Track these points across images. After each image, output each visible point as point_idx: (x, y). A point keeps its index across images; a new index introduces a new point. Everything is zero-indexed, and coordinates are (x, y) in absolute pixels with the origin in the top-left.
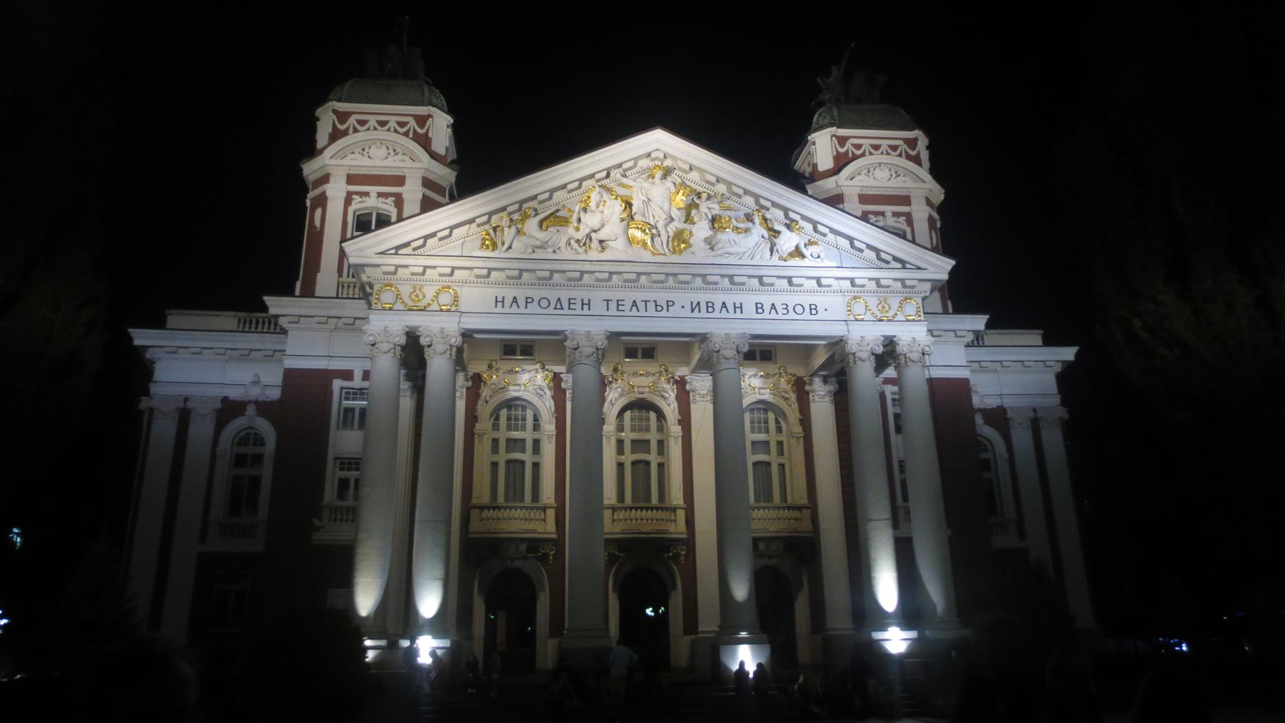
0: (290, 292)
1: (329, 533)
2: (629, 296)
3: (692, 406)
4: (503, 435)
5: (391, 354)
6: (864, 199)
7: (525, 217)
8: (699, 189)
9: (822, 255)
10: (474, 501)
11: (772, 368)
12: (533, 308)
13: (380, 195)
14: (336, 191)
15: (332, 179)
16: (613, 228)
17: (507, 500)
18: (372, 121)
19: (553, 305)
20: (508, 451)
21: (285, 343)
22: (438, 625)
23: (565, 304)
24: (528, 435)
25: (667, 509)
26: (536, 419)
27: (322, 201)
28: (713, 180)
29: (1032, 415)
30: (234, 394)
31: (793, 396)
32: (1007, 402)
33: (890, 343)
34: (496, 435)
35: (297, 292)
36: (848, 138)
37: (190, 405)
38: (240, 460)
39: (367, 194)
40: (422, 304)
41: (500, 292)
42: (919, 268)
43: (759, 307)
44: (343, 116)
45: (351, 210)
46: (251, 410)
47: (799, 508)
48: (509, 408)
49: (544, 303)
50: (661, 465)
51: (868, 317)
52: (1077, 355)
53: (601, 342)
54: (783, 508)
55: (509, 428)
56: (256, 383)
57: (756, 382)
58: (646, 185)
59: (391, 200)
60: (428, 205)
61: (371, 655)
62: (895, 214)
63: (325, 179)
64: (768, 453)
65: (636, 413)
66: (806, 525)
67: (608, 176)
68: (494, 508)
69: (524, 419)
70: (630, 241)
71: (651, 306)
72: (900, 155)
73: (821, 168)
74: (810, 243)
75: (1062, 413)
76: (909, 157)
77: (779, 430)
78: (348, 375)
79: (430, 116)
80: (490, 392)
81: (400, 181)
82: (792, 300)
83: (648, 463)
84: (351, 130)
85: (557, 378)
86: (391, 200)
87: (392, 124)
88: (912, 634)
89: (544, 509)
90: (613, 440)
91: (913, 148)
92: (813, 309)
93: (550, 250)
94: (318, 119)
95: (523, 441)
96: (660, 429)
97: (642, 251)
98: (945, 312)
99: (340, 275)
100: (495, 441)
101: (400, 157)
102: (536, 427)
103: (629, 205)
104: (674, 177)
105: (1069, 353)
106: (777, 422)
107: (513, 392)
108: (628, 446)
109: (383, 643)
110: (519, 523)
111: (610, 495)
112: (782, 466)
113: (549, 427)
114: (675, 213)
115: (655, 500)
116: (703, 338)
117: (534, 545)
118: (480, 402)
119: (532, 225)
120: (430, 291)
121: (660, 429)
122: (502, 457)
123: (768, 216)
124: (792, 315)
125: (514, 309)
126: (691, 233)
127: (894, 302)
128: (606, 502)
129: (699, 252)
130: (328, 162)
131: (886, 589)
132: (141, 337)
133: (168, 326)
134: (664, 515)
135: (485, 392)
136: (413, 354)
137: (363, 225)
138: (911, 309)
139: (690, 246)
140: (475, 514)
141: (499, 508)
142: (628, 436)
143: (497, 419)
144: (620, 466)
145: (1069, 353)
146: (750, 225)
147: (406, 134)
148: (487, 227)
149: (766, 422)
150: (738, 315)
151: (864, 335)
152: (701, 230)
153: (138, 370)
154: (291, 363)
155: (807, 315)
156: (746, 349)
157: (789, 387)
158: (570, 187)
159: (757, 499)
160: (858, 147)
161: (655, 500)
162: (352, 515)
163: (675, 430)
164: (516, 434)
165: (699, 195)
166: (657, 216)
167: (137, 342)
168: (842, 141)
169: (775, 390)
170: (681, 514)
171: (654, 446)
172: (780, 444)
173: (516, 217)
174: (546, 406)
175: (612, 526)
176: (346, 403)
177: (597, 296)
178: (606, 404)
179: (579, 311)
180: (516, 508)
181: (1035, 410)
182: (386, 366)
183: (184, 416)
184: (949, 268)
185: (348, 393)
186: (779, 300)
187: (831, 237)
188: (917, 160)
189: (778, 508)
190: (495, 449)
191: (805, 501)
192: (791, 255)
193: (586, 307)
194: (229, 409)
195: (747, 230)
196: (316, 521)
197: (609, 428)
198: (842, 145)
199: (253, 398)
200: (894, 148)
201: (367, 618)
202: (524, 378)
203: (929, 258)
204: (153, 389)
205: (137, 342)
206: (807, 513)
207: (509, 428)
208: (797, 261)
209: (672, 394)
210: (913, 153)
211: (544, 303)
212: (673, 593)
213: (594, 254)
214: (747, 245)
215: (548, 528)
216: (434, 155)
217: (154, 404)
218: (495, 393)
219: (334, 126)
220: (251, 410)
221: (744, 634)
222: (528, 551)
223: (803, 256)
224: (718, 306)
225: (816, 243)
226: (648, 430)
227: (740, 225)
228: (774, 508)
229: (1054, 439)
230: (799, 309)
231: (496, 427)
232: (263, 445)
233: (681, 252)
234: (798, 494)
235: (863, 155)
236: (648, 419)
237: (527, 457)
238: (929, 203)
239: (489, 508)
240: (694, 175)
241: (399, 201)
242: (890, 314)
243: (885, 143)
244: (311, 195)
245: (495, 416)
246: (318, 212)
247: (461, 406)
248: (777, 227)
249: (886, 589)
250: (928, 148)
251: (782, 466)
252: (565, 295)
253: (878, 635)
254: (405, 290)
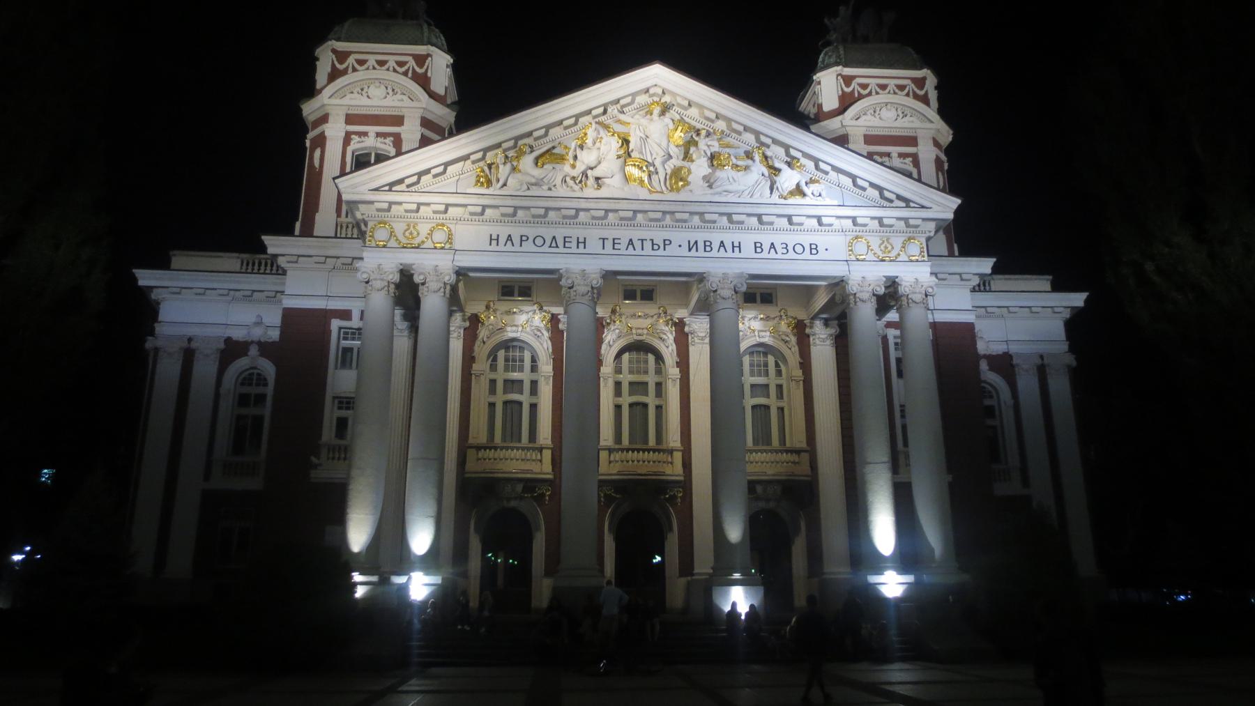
0: (289, 232)
1: (325, 471)
2: (625, 234)
3: (691, 349)
4: (500, 376)
5: (384, 292)
6: (869, 139)
7: (521, 154)
8: (699, 126)
9: (823, 194)
10: (471, 441)
11: (772, 310)
12: (528, 246)
13: (378, 135)
14: (335, 131)
15: (331, 119)
16: (610, 166)
17: (504, 440)
18: (372, 60)
19: (548, 243)
20: (505, 392)
21: (284, 284)
22: (430, 561)
23: (560, 243)
24: (525, 376)
25: (664, 451)
26: (534, 360)
27: (321, 141)
28: (713, 116)
29: (1039, 362)
30: (238, 335)
31: (793, 339)
32: (1013, 349)
33: (892, 284)
34: (493, 376)
35: (297, 232)
36: (853, 77)
37: (194, 345)
38: (243, 400)
39: (365, 134)
40: (416, 242)
41: (495, 230)
42: (923, 207)
43: (758, 246)
44: (342, 56)
45: (349, 150)
46: (254, 351)
47: (798, 452)
48: (507, 349)
49: (539, 241)
50: (659, 408)
51: (870, 257)
52: (1086, 301)
53: (597, 281)
54: (782, 452)
55: (506, 369)
56: (259, 323)
57: (756, 325)
58: (644, 121)
59: (389, 140)
60: (425, 142)
61: (360, 592)
62: (901, 155)
63: (324, 119)
64: (768, 396)
65: (635, 355)
66: (805, 468)
67: (605, 112)
68: (490, 448)
69: (522, 360)
70: (627, 179)
71: (648, 245)
72: (908, 95)
73: (826, 108)
74: (812, 181)
75: (1071, 360)
76: (916, 97)
77: (779, 373)
78: (345, 315)
79: (429, 55)
80: (487, 333)
81: (398, 120)
82: (791, 239)
83: (645, 405)
84: (350, 70)
85: (554, 319)
86: (389, 140)
87: (392, 64)
88: (909, 578)
89: (541, 450)
90: (611, 383)
91: (921, 88)
92: (814, 248)
93: (545, 187)
94: (317, 59)
95: (521, 382)
96: (659, 371)
97: (639, 188)
98: (951, 254)
99: (339, 215)
100: (493, 382)
101: (399, 96)
102: (534, 368)
103: (626, 142)
104: (673, 113)
105: (1078, 299)
106: (777, 365)
107: (510, 333)
108: (625, 388)
109: (374, 579)
111: (606, 435)
112: (781, 409)
113: (546, 368)
114: (674, 151)
115: (652, 442)
116: (701, 278)
117: (531, 485)
118: (478, 343)
119: (527, 162)
120: (424, 229)
121: (659, 371)
122: (500, 398)
123: (769, 153)
124: (791, 255)
125: (509, 247)
126: (689, 171)
127: (897, 242)
128: (602, 443)
129: (696, 190)
130: (326, 101)
131: (883, 532)
132: (146, 278)
133: (173, 266)
134: (662, 456)
135: (483, 333)
136: (407, 291)
137: (362, 162)
138: (915, 249)
139: (688, 184)
140: (471, 454)
141: (496, 448)
142: (626, 378)
143: (495, 359)
144: (618, 408)
145: (1078, 299)
146: (750, 162)
147: (405, 74)
148: (481, 164)
149: (766, 365)
150: (737, 254)
151: (866, 276)
152: (700, 167)
153: (144, 310)
154: (290, 303)
155: (807, 255)
156: (744, 289)
157: (789, 330)
158: (566, 123)
159: (756, 442)
160: (864, 86)
161: (652, 442)
162: (343, 453)
163: (674, 372)
164: (515, 375)
165: (698, 132)
166: (655, 153)
167: (141, 283)
168: (848, 80)
169: (775, 332)
170: (678, 456)
171: (652, 389)
172: (780, 387)
173: (511, 154)
174: (543, 347)
175: (609, 467)
176: (345, 343)
177: (593, 235)
178: (604, 346)
179: (574, 250)
180: (512, 449)
181: (1042, 357)
182: (380, 302)
183: (189, 355)
184: (955, 207)
185: (346, 333)
186: (778, 239)
187: (833, 174)
188: (925, 100)
189: (777, 451)
190: (493, 390)
191: (804, 445)
192: (792, 193)
193: (581, 246)
194: (232, 350)
195: (747, 168)
196: (313, 459)
197: (607, 369)
198: (848, 85)
199: (256, 339)
200: (901, 88)
201: (359, 554)
202: (522, 319)
203: (934, 197)
204: (158, 328)
205: (141, 283)
206: (805, 456)
207: (506, 369)
208: (798, 200)
210: (922, 93)
211: (539, 241)
212: (669, 536)
213: (590, 192)
214: (746, 183)
215: (544, 468)
216: (432, 95)
217: (159, 343)
218: (492, 333)
219: (333, 65)
220: (254, 351)
221: (737, 576)
222: (525, 490)
223: (804, 195)
224: (716, 245)
225: (817, 182)
226: (646, 372)
227: (740, 163)
228: (771, 451)
229: (1060, 386)
230: (799, 249)
231: (493, 368)
232: (266, 385)
233: (678, 190)
234: (797, 438)
235: (870, 94)
236: (646, 362)
237: (525, 398)
238: (936, 144)
239: (485, 448)
240: (694, 112)
241: (397, 140)
242: (893, 254)
243: (892, 82)
244: (310, 135)
245: (493, 356)
246: (317, 153)
247: (457, 346)
248: (777, 165)
249: (883, 532)
250: (936, 88)
251: (781, 409)
252: (560, 233)
253: (873, 579)
254: (399, 227)
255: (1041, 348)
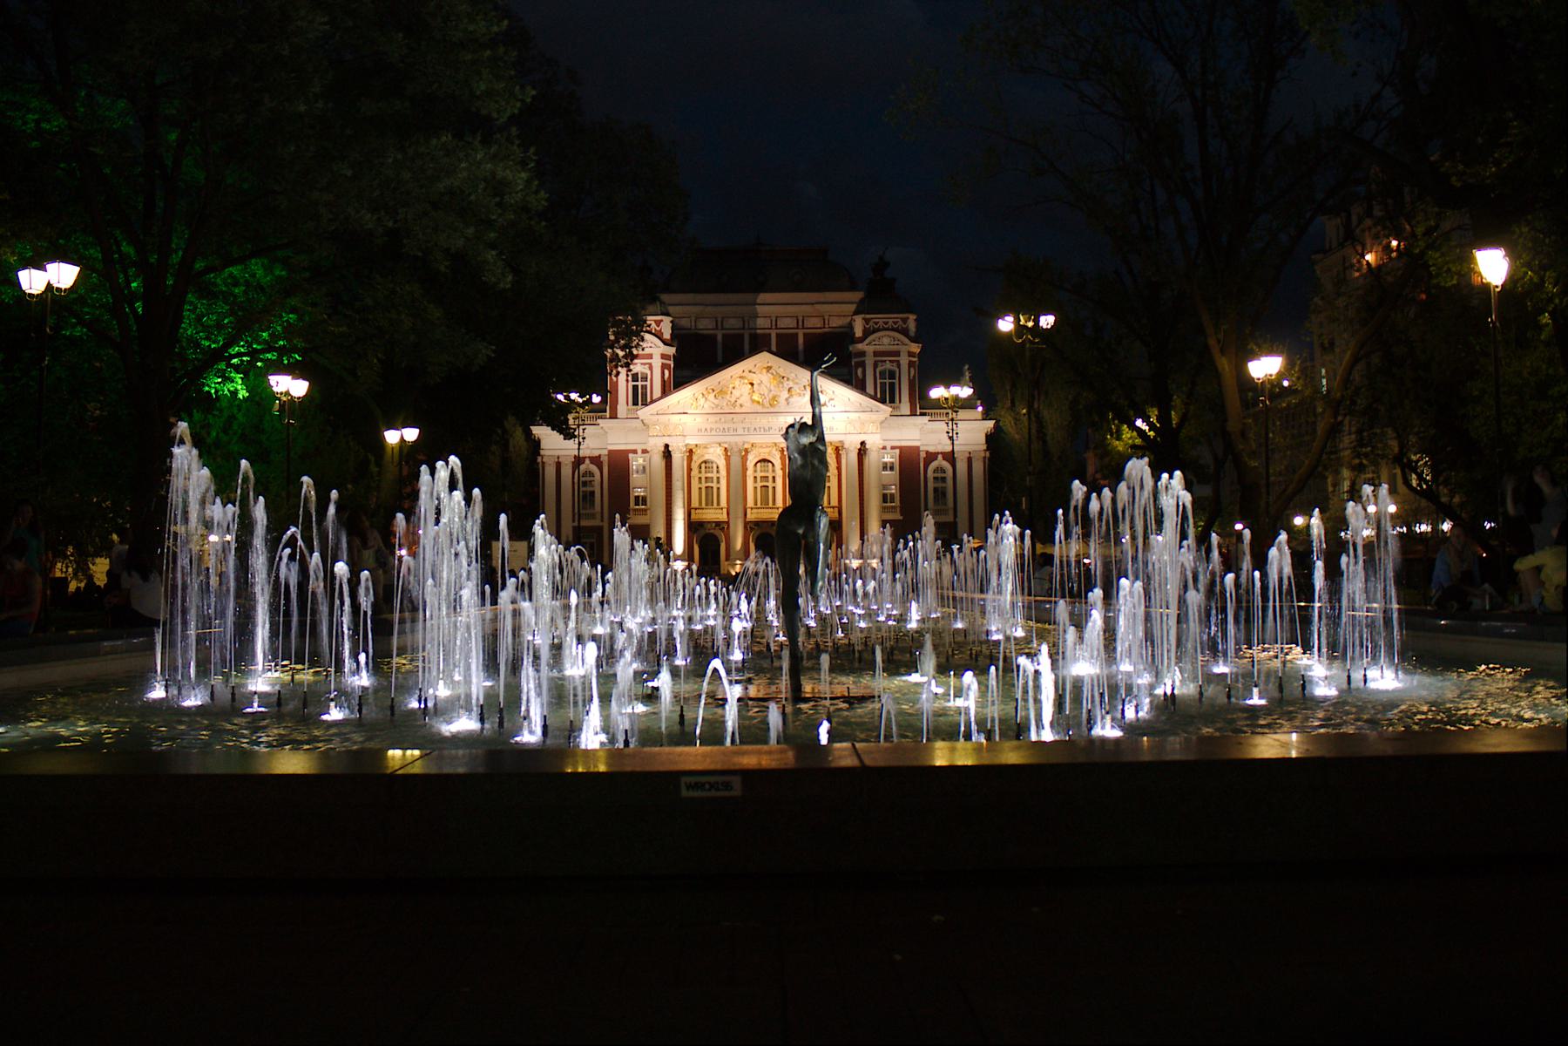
4: (703, 476)
24: (714, 475)
78: (635, 452)
98: (913, 414)
107: (707, 457)
110: (711, 515)
111: (750, 503)
113: (723, 473)
117: (718, 524)
119: (711, 397)
122: (704, 485)
142: (759, 474)
152: (785, 394)
168: (867, 321)
174: (722, 463)
175: (751, 516)
183: (558, 465)
197: (750, 473)
209: (778, 455)
215: (724, 517)
216: (665, 342)
229: (978, 468)
235: (878, 330)
237: (714, 485)
255: (969, 448)
